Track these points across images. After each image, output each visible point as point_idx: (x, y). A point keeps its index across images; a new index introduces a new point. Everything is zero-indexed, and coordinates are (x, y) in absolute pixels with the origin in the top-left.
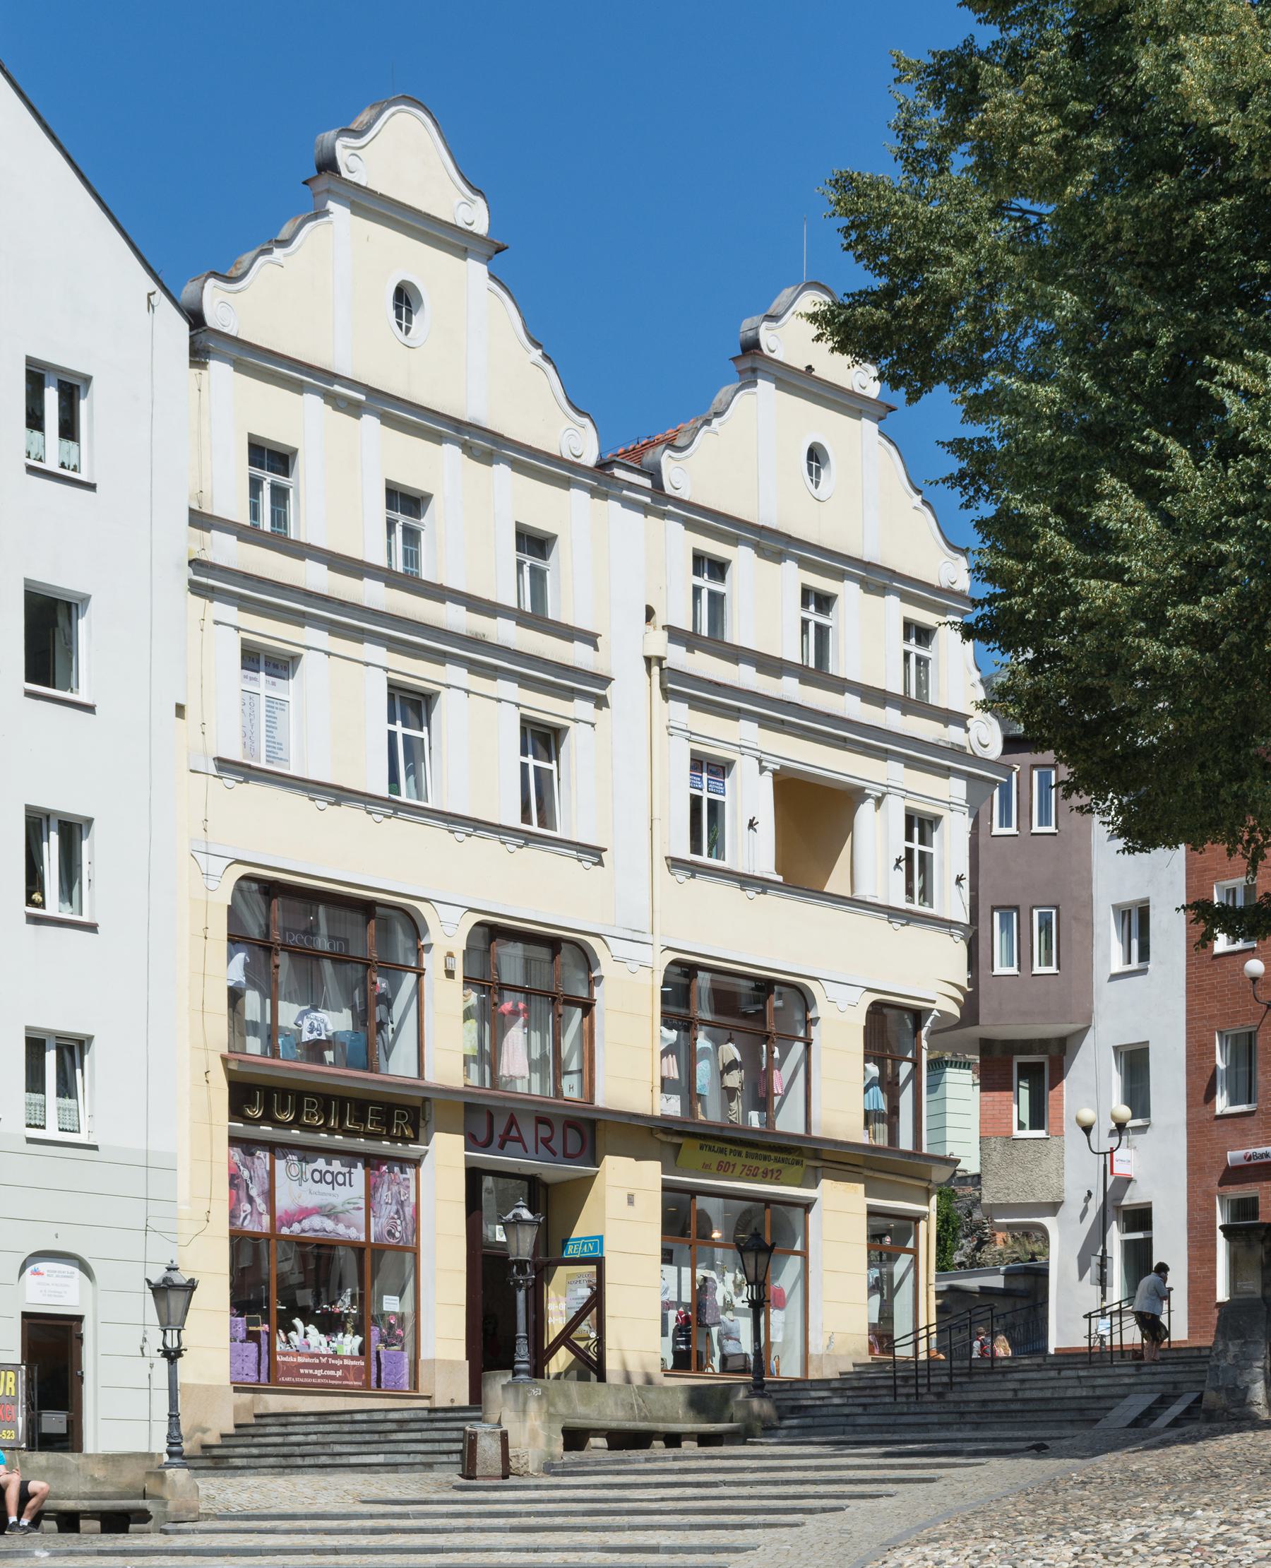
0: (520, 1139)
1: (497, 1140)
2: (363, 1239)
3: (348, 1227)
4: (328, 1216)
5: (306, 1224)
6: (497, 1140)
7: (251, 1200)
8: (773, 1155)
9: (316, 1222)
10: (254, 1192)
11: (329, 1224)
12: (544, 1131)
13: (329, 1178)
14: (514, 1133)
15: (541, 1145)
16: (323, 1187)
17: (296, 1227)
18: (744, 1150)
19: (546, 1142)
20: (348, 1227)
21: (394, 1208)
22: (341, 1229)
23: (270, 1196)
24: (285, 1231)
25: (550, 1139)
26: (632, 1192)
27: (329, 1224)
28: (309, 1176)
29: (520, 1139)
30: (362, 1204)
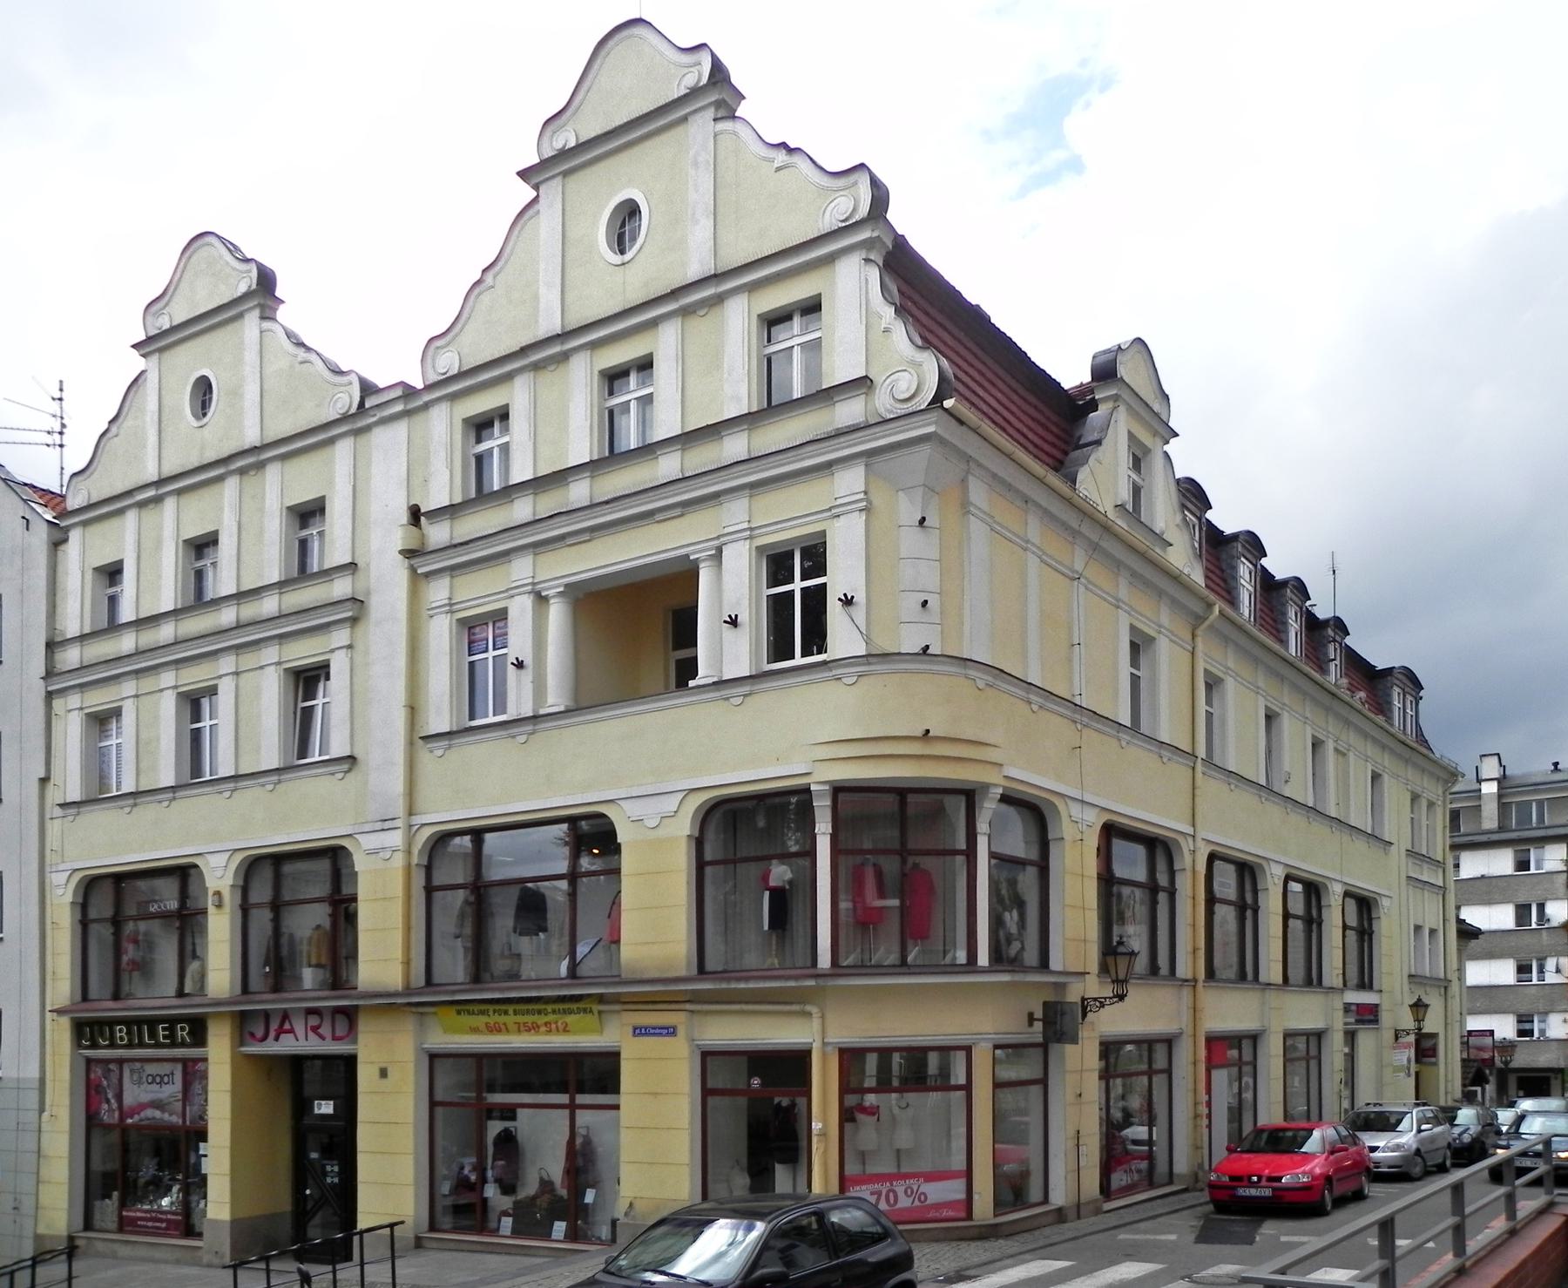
0: (291, 1031)
1: (272, 1034)
6: (272, 1034)
7: (108, 1101)
8: (549, 1008)
9: (149, 1113)
10: (110, 1096)
11: (157, 1114)
12: (314, 1021)
14: (287, 1026)
15: (310, 1034)
16: (155, 1087)
18: (511, 1008)
19: (315, 1029)
22: (166, 1116)
23: (119, 1097)
24: (130, 1121)
25: (319, 1027)
30: (180, 1096)
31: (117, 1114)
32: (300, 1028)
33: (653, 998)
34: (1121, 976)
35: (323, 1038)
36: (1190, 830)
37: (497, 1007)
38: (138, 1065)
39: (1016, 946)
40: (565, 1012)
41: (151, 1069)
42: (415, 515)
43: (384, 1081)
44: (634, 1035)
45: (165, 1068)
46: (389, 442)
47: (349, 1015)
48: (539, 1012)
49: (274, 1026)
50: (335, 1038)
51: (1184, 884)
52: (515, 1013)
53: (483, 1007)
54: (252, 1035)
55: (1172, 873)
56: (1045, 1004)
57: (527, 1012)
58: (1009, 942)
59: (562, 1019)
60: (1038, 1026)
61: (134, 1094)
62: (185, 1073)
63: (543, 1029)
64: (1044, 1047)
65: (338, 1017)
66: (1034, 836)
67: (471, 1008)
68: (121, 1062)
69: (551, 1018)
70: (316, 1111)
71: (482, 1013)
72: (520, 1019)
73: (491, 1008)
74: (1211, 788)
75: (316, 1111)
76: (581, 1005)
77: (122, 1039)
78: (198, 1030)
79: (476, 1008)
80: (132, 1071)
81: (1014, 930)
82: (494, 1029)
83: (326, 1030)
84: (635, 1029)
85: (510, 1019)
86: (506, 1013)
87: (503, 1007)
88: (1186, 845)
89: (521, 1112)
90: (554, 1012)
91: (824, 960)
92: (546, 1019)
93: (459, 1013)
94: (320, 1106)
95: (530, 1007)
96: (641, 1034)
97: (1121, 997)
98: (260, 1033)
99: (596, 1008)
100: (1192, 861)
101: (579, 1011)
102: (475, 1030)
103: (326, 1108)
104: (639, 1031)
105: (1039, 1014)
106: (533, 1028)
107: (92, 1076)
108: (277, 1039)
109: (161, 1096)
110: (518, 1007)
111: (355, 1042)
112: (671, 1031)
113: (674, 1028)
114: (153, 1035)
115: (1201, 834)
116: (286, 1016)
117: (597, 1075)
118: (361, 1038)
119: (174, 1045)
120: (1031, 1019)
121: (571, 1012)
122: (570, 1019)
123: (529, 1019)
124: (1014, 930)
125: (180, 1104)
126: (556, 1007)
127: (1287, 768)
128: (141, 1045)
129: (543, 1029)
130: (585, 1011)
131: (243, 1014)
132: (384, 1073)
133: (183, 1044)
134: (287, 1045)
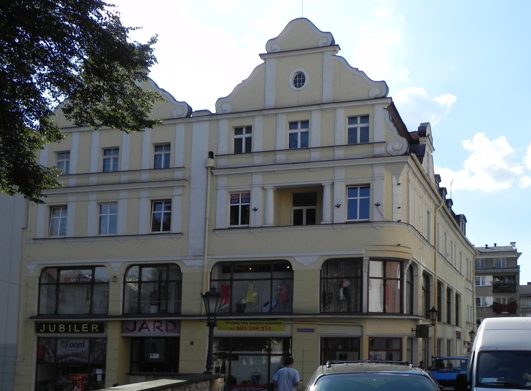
1: (137, 329)
2: (87, 361)
3: (82, 359)
4: (75, 356)
5: (67, 359)
7: (49, 354)
8: (264, 322)
9: (71, 358)
10: (50, 351)
11: (75, 358)
12: (157, 324)
13: (76, 345)
14: (145, 326)
15: (156, 329)
16: (74, 348)
17: (64, 360)
18: (249, 322)
19: (158, 328)
20: (82, 359)
21: (100, 352)
22: (80, 359)
23: (55, 352)
24: (60, 361)
25: (161, 326)
27: (75, 358)
28: (69, 345)
29: (147, 328)
30: (88, 352)
31: (53, 358)
32: (151, 326)
33: (308, 319)
35: (162, 331)
37: (243, 321)
38: (66, 340)
40: (270, 323)
41: (71, 341)
43: (192, 346)
44: (298, 331)
45: (81, 341)
47: (177, 325)
48: (260, 323)
49: (138, 325)
52: (250, 323)
53: (238, 321)
54: (128, 329)
57: (256, 323)
59: (268, 326)
61: (61, 351)
62: (91, 342)
63: (261, 329)
67: (231, 321)
68: (56, 339)
71: (236, 323)
72: (252, 325)
73: (240, 322)
76: (277, 321)
78: (102, 327)
79: (234, 321)
80: (62, 343)
82: (238, 329)
83: (163, 327)
84: (298, 330)
86: (246, 323)
90: (266, 323)
92: (263, 326)
93: (226, 323)
95: (257, 322)
96: (300, 331)
98: (131, 327)
99: (283, 322)
101: (276, 323)
104: (299, 330)
106: (257, 329)
107: (40, 344)
108: (140, 331)
110: (251, 322)
111: (179, 332)
112: (312, 331)
113: (313, 330)
116: (144, 322)
119: (90, 331)
121: (273, 324)
122: (271, 326)
123: (255, 326)
125: (87, 355)
126: (267, 322)
130: (279, 323)
132: (192, 343)
133: (95, 331)
134: (144, 333)
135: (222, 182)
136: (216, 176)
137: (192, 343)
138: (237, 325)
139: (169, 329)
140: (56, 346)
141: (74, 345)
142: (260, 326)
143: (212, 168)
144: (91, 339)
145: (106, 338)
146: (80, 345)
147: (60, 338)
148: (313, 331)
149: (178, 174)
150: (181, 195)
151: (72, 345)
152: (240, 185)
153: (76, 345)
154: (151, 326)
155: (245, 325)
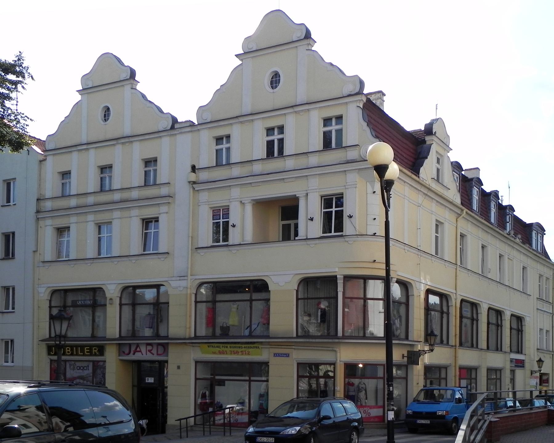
0: (140, 351)
1: (132, 352)
6: (132, 352)
8: (243, 346)
12: (149, 348)
13: (82, 368)
14: (138, 349)
15: (148, 352)
16: (80, 371)
18: (229, 346)
19: (150, 351)
23: (65, 374)
25: (152, 350)
26: (179, 365)
29: (140, 351)
30: (91, 375)
34: (432, 343)
35: (153, 354)
36: (454, 292)
37: (223, 345)
38: (73, 362)
39: (399, 331)
41: (78, 364)
42: (194, 169)
43: (179, 370)
45: (85, 364)
46: (184, 140)
47: (165, 347)
48: (239, 347)
49: (133, 349)
50: (158, 354)
51: (452, 311)
53: (219, 345)
54: (124, 352)
55: (448, 307)
56: (408, 351)
57: (235, 347)
58: (397, 330)
59: (247, 350)
60: (406, 359)
62: (94, 366)
63: (240, 353)
64: (406, 366)
65: (159, 347)
66: (404, 294)
69: (243, 349)
70: (147, 381)
71: (218, 347)
72: (232, 349)
73: (221, 345)
74: (462, 274)
75: (147, 381)
76: (255, 345)
77: (68, 352)
78: (101, 350)
81: (398, 326)
82: (220, 353)
83: (154, 351)
84: (274, 354)
85: (228, 350)
86: (227, 347)
87: (226, 345)
88: (453, 297)
89: (226, 382)
90: (245, 347)
91: (340, 334)
93: (209, 347)
94: (148, 379)
96: (276, 356)
97: (432, 350)
98: (127, 351)
99: (260, 346)
100: (455, 303)
101: (254, 347)
102: (214, 353)
103: (151, 380)
104: (276, 355)
105: (406, 355)
106: (237, 353)
107: (53, 366)
108: (134, 354)
109: (82, 374)
111: (167, 356)
112: (287, 355)
114: (82, 351)
115: (458, 293)
116: (138, 345)
117: (258, 370)
118: (170, 354)
119: (91, 355)
120: (403, 356)
121: (251, 348)
122: (250, 350)
123: (235, 350)
124: (398, 326)
126: (246, 346)
127: (489, 266)
128: (77, 355)
129: (240, 353)
130: (256, 347)
131: (119, 344)
132: (179, 367)
133: (95, 355)
134: (138, 356)
135: (204, 196)
136: (198, 190)
137: (179, 367)
138: (218, 349)
139: (159, 353)
140: (65, 369)
141: (80, 368)
142: (240, 350)
143: (194, 183)
144: (93, 362)
145: (105, 361)
146: (85, 368)
147: (68, 361)
148: (288, 356)
149: (164, 191)
150: (167, 213)
151: (78, 368)
152: (219, 199)
153: (82, 368)
154: (143, 349)
155: (226, 349)
